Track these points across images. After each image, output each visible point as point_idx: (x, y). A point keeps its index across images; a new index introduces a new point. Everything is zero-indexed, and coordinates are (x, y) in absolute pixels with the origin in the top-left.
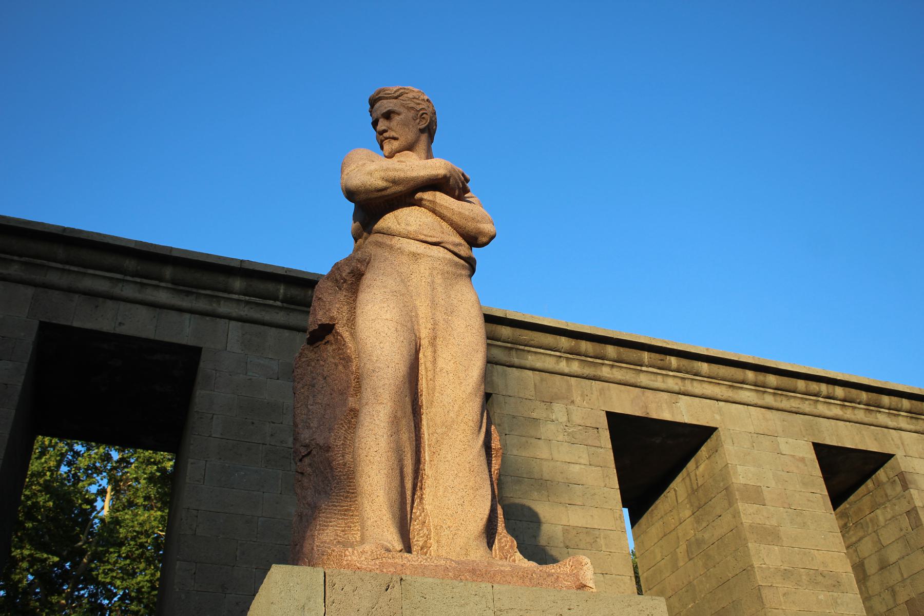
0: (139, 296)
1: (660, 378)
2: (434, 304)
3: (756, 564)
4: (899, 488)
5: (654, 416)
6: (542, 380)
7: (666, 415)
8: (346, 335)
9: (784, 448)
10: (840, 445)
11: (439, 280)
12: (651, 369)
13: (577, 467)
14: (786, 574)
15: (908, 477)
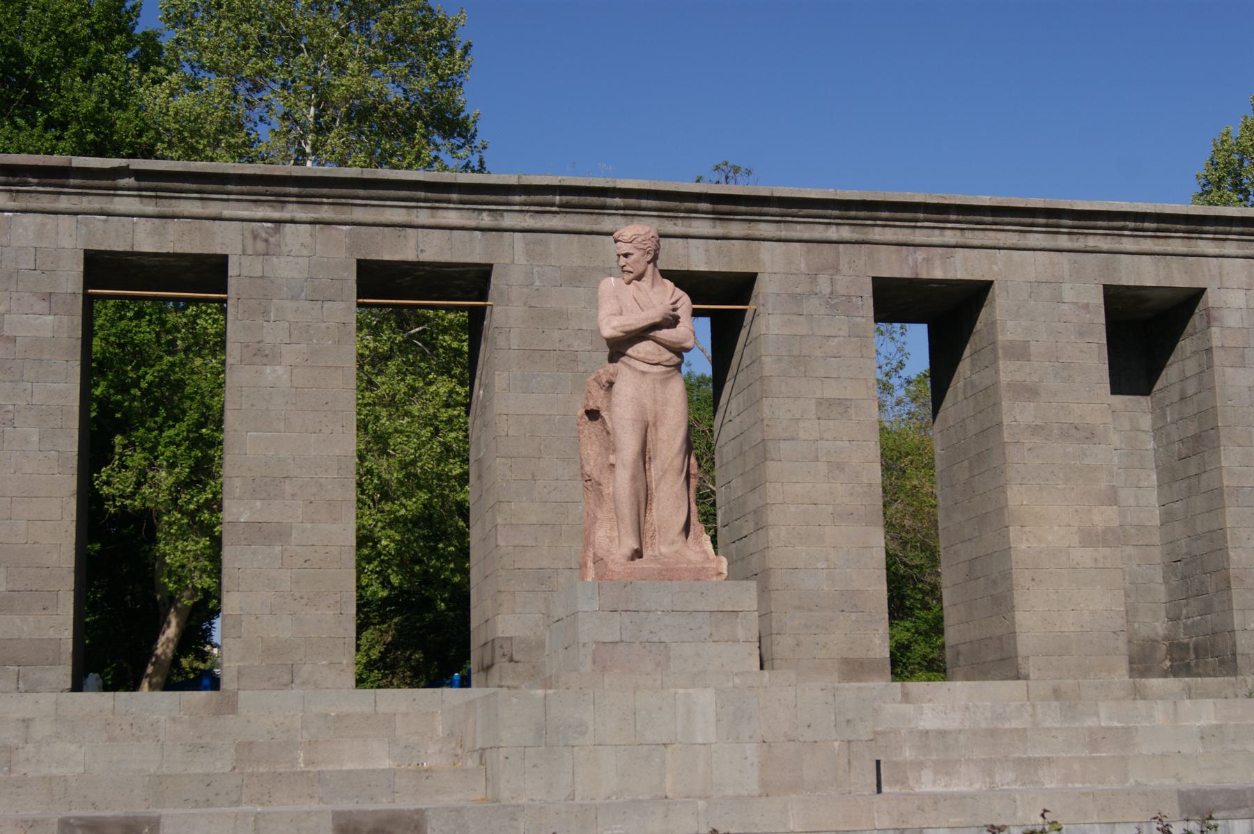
0: (431, 221)
1: (937, 232)
2: (655, 402)
3: (1006, 420)
4: (1204, 324)
5: (924, 275)
6: (809, 251)
7: (938, 274)
8: (606, 417)
9: (1068, 294)
10: (1138, 284)
11: (658, 385)
12: (926, 224)
13: (836, 340)
14: (1035, 430)
15: (1215, 314)
